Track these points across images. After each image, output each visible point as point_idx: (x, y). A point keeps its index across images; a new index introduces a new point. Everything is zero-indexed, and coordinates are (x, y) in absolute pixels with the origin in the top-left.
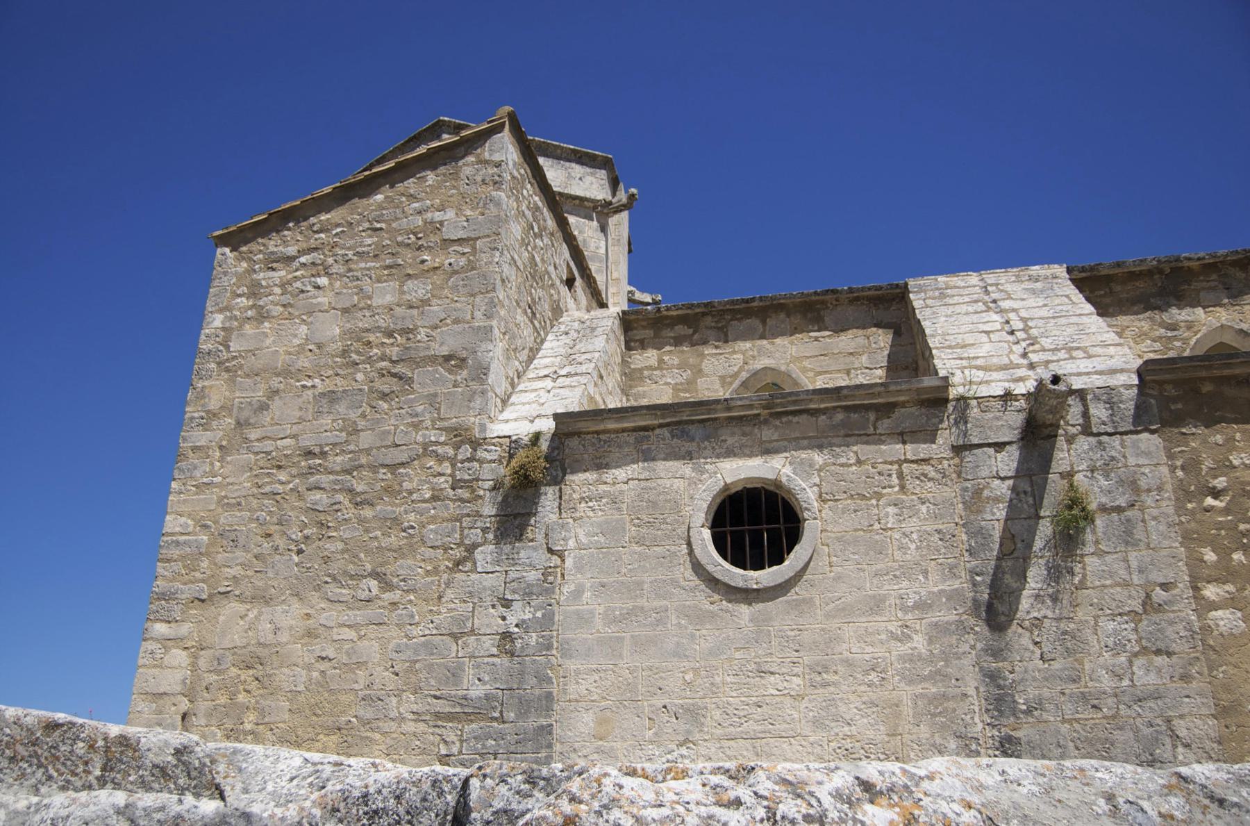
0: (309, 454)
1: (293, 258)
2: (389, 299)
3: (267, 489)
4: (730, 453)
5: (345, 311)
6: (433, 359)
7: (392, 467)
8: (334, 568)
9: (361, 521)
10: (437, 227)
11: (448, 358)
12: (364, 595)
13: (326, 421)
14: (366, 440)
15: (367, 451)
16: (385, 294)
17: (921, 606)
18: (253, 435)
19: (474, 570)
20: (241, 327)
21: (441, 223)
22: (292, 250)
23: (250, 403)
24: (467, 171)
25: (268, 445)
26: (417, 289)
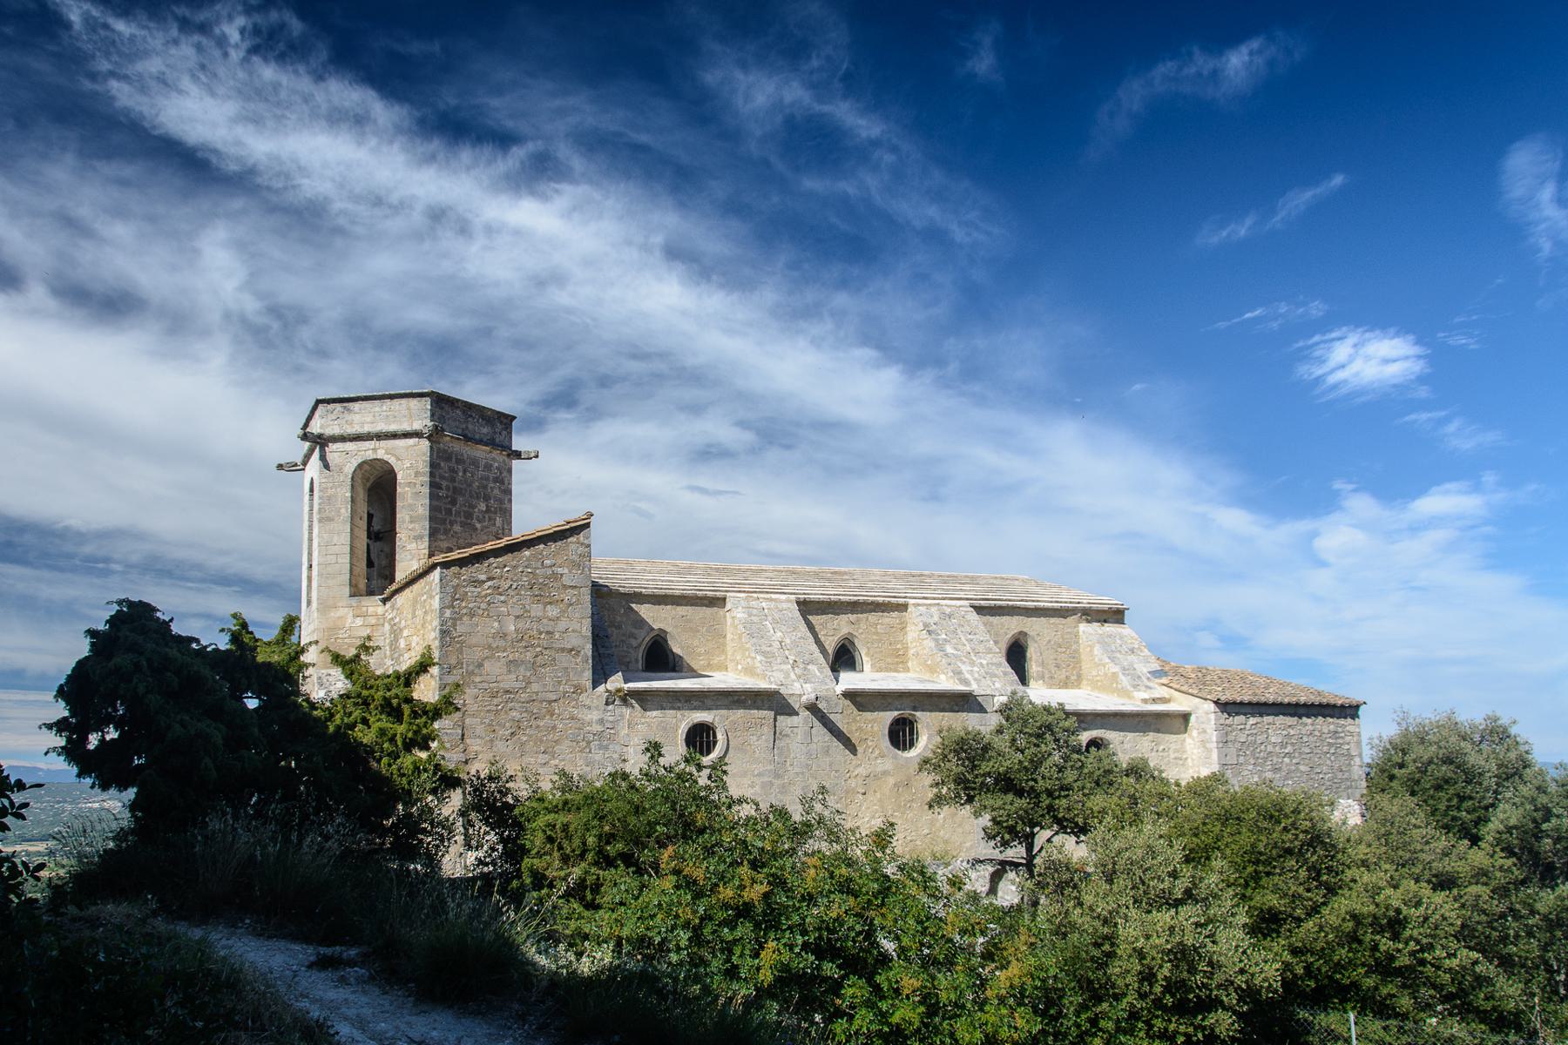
0: (507, 692)
1: (484, 582)
2: (540, 614)
3: (488, 708)
4: (696, 708)
5: (517, 617)
6: (563, 650)
7: (550, 702)
8: (527, 748)
9: (538, 727)
10: (556, 577)
11: (572, 650)
12: (543, 761)
13: (513, 676)
14: (535, 687)
15: (537, 693)
16: (536, 610)
17: (759, 775)
18: (478, 679)
19: (590, 752)
20: (461, 619)
21: (562, 575)
22: (483, 577)
23: (473, 663)
24: (573, 547)
25: (485, 685)
26: (552, 611)
